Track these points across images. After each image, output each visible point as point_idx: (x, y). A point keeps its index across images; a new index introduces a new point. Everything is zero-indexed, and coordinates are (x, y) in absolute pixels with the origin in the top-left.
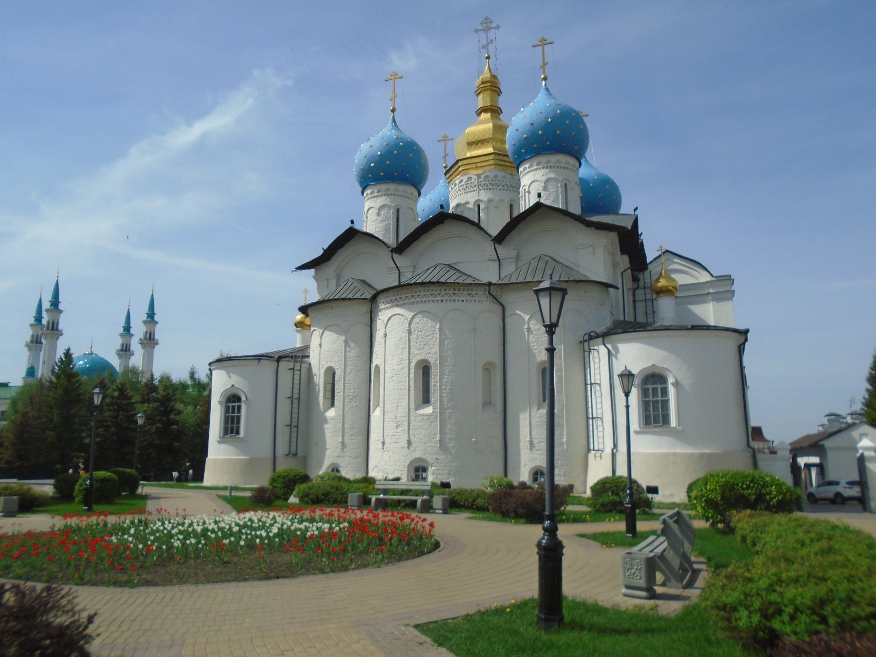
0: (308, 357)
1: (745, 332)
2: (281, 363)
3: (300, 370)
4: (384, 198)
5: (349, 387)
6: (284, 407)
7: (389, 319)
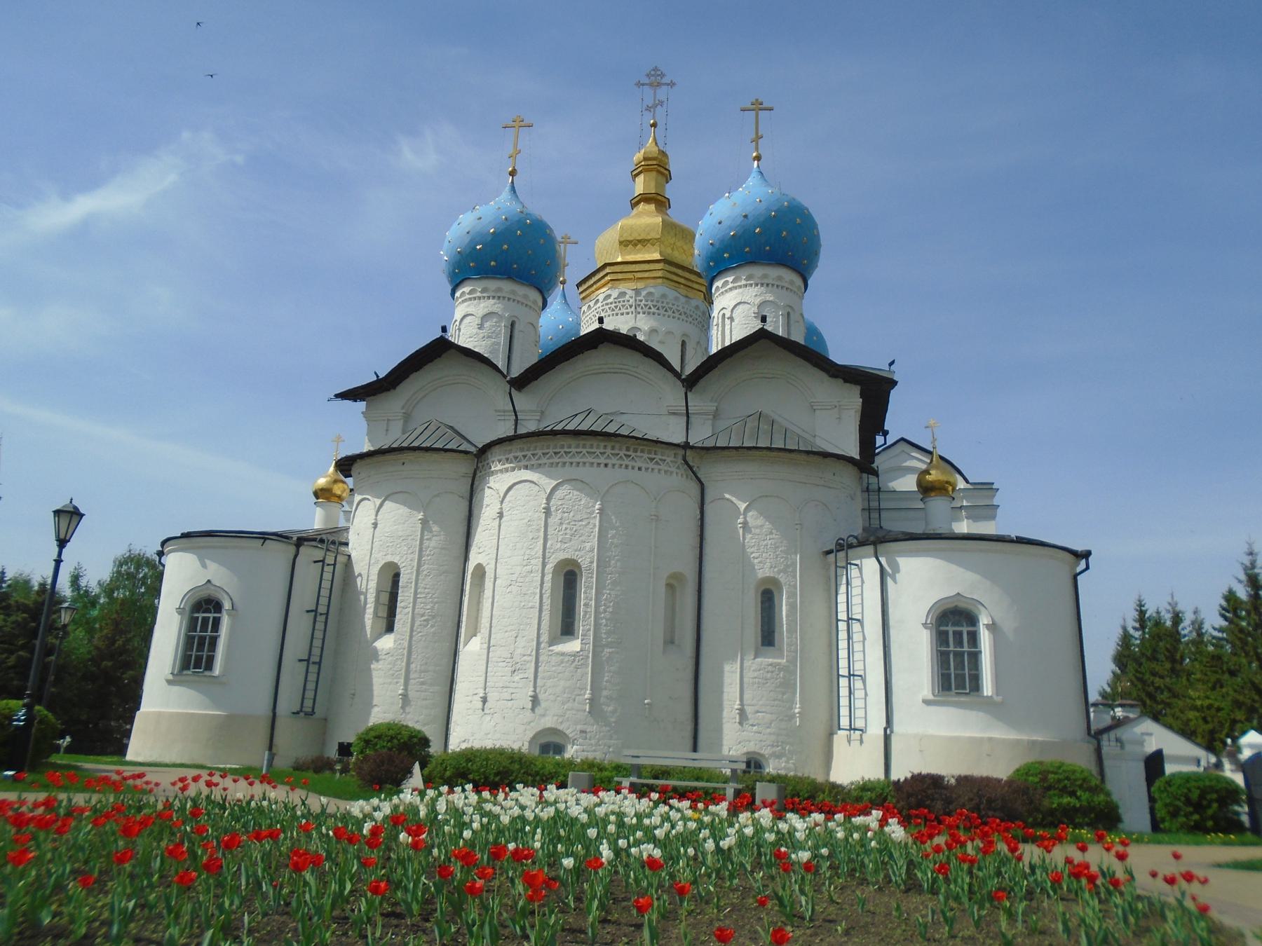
0: (347, 544)
1: (1086, 555)
2: (302, 549)
3: (334, 565)
4: (492, 301)
5: (423, 600)
6: (300, 626)
7: (510, 488)
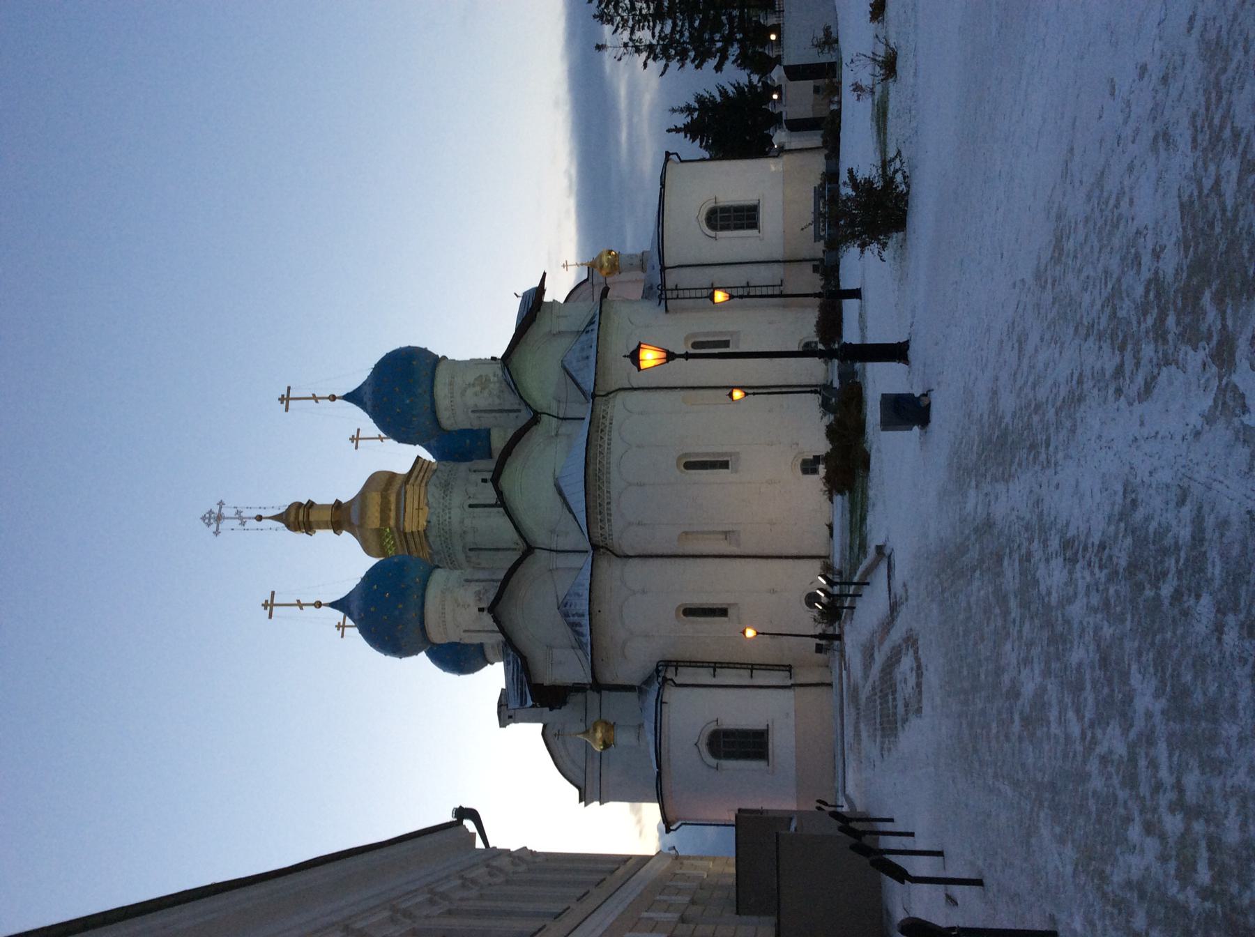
1: (668, 154)
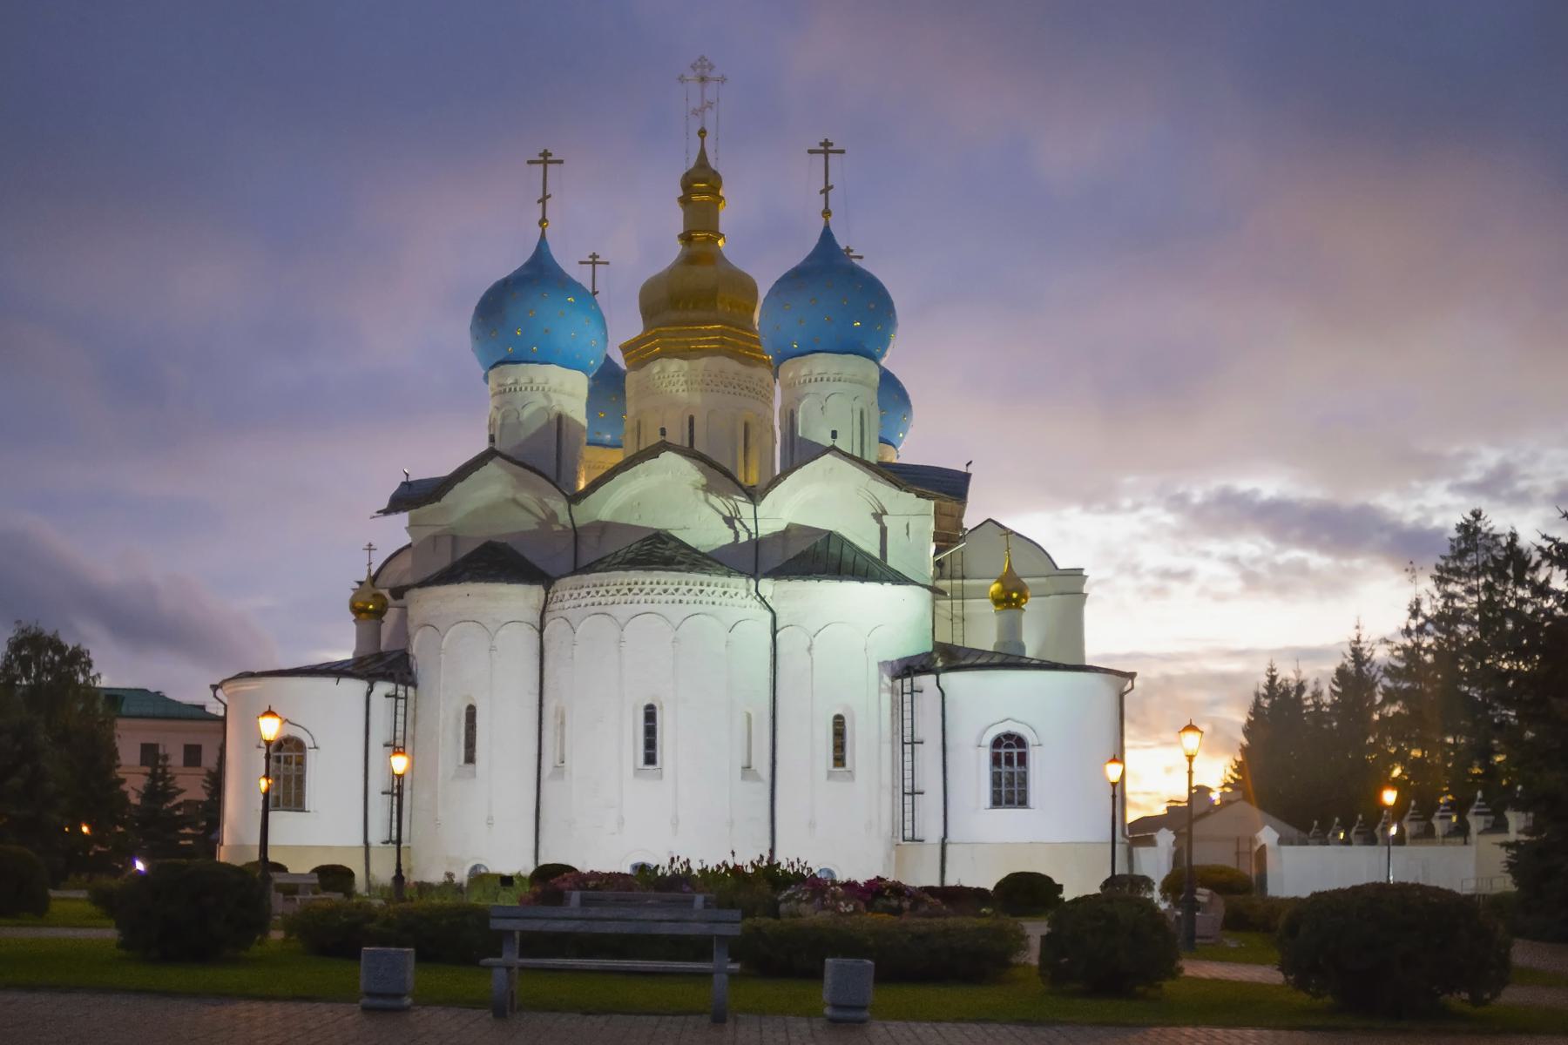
1: (1132, 676)
